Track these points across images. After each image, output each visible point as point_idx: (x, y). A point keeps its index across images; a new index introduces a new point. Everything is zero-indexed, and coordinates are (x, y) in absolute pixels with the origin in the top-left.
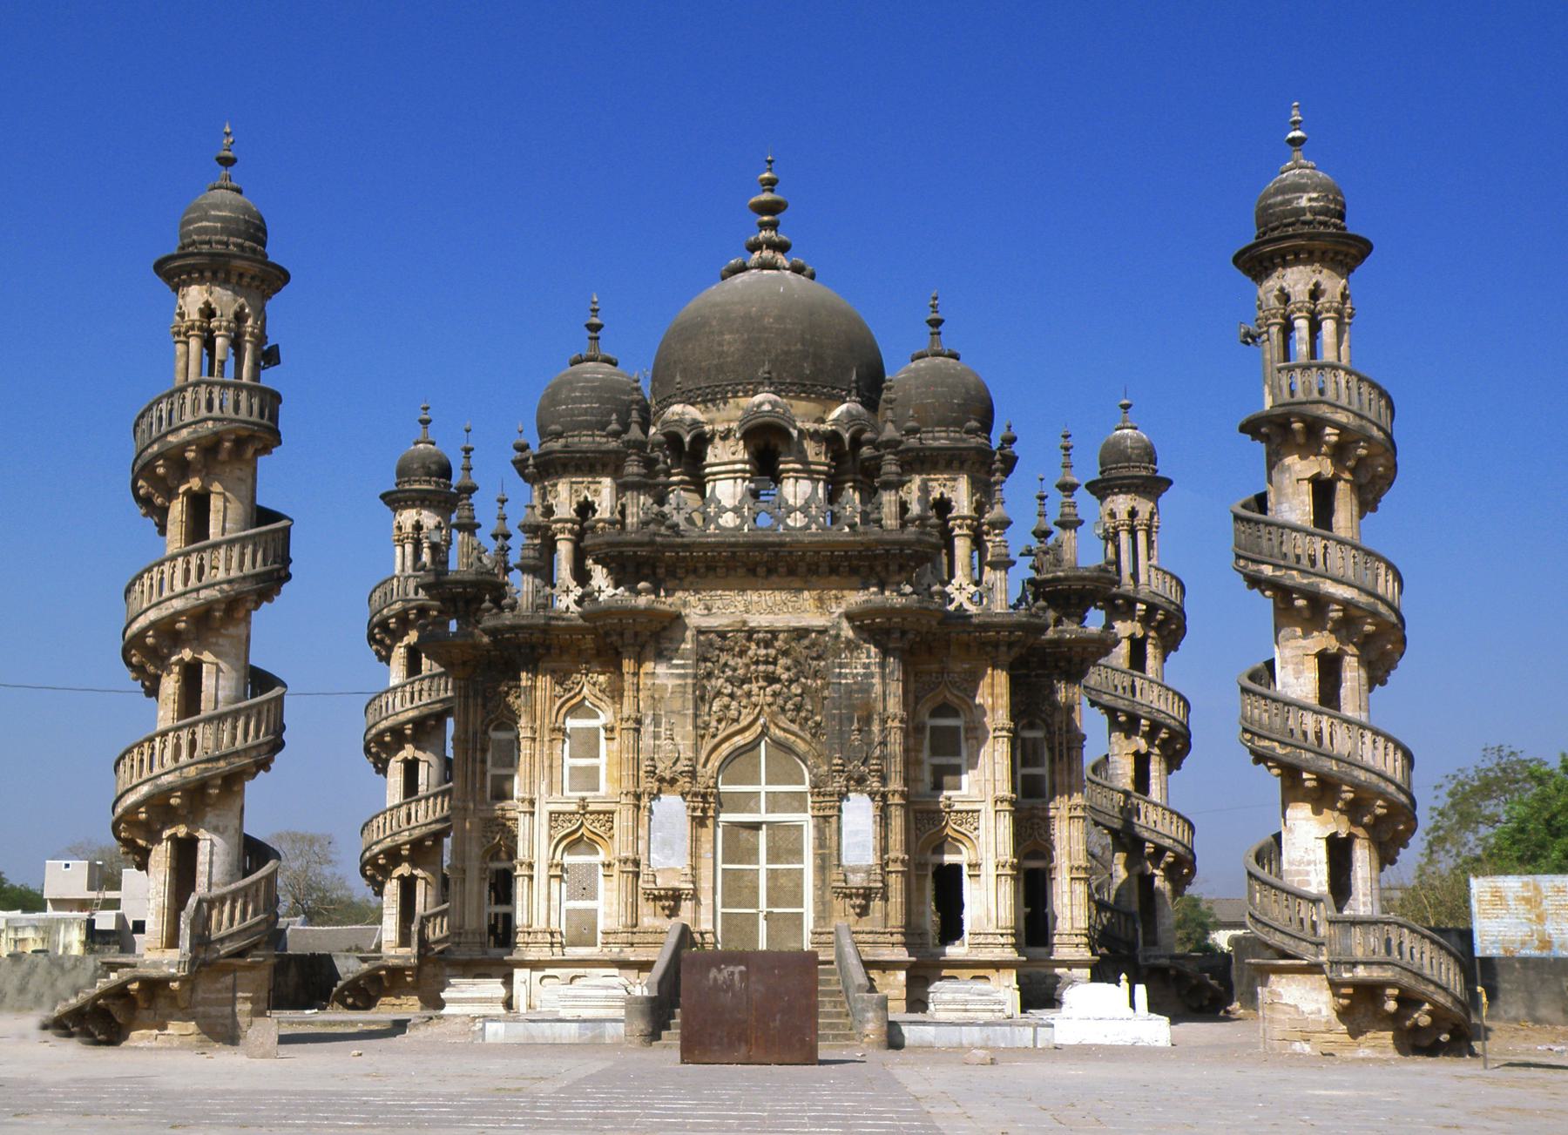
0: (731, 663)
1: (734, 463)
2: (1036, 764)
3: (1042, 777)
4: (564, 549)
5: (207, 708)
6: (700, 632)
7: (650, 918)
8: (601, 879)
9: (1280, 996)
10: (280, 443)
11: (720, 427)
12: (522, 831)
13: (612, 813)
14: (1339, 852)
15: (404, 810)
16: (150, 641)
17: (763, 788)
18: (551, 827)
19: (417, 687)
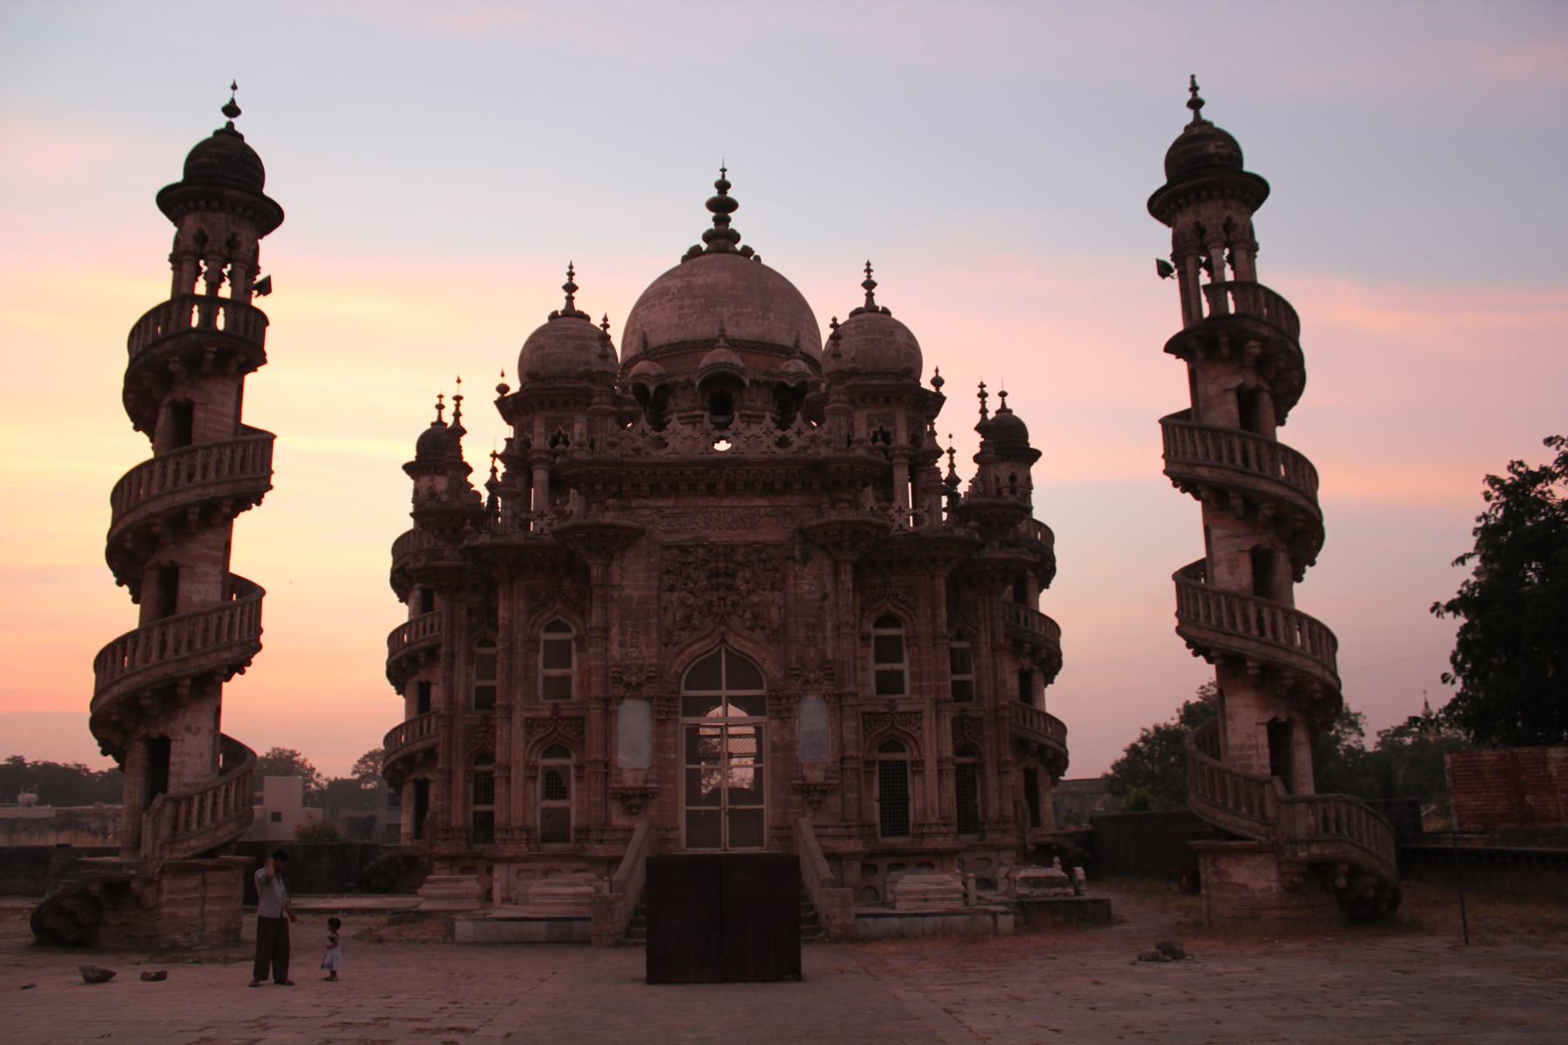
0: (694, 575)
1: (694, 409)
2: (964, 672)
3: (969, 682)
4: (540, 476)
5: (182, 610)
6: (667, 547)
7: (618, 820)
8: (573, 780)
9: (1230, 875)
10: (264, 362)
11: (681, 379)
12: (501, 733)
13: (583, 718)
14: (1278, 735)
15: (417, 725)
16: (129, 545)
17: (724, 693)
18: (529, 733)
19: (429, 622)
